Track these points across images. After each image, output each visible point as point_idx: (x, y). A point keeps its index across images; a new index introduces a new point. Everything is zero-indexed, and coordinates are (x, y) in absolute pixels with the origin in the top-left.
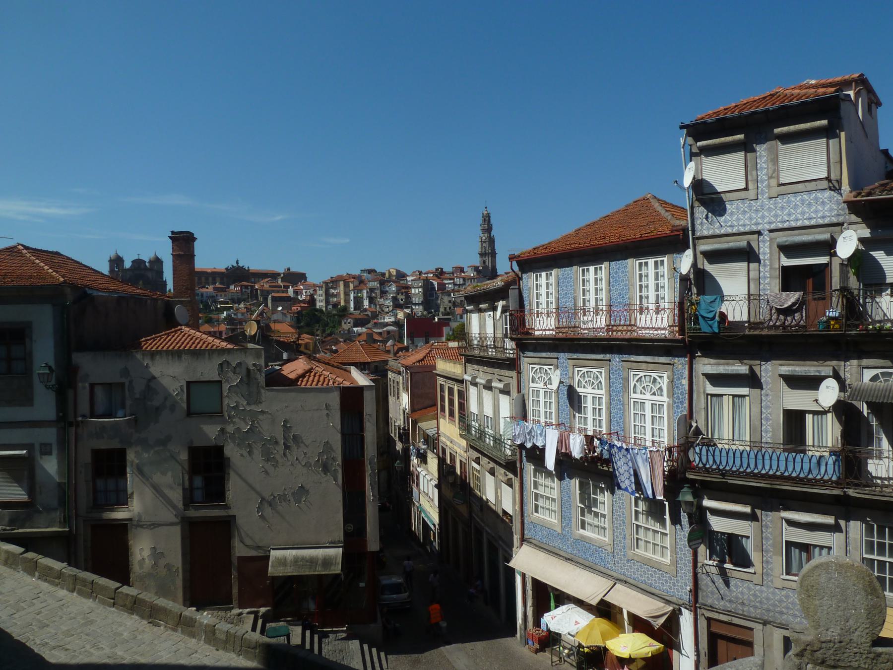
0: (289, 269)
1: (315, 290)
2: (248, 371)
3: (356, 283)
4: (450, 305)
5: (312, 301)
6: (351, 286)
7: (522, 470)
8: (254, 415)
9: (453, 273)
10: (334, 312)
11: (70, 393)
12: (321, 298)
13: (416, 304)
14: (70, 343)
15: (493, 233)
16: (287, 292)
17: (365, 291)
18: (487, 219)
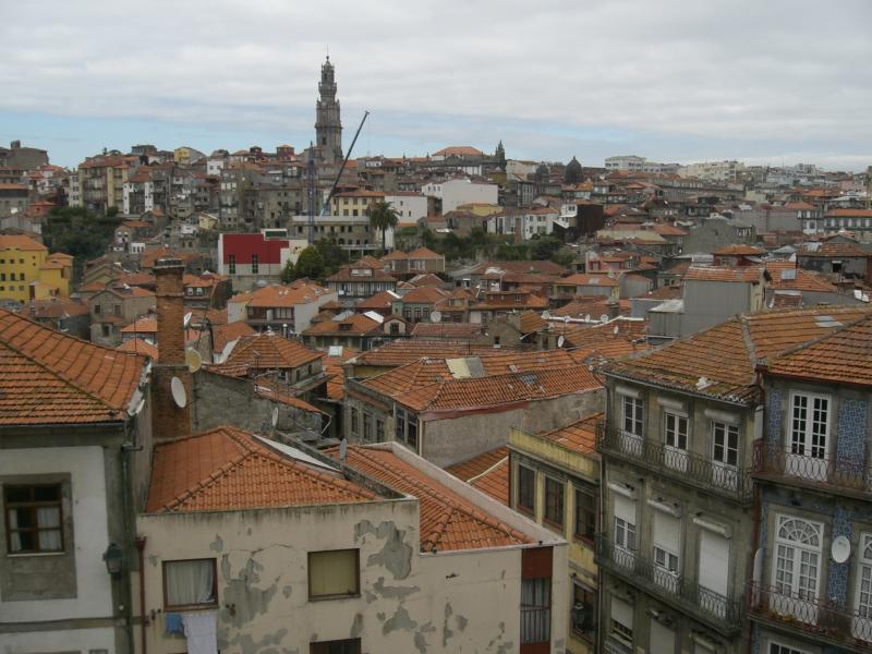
1: (66, 181)
2: (398, 533)
3: (132, 170)
4: (280, 208)
5: (59, 198)
6: (125, 174)
8: (402, 594)
9: (276, 156)
10: (99, 216)
11: (135, 578)
12: (77, 193)
13: (227, 206)
14: (126, 504)
15: (337, 97)
16: (18, 179)
18: (328, 73)
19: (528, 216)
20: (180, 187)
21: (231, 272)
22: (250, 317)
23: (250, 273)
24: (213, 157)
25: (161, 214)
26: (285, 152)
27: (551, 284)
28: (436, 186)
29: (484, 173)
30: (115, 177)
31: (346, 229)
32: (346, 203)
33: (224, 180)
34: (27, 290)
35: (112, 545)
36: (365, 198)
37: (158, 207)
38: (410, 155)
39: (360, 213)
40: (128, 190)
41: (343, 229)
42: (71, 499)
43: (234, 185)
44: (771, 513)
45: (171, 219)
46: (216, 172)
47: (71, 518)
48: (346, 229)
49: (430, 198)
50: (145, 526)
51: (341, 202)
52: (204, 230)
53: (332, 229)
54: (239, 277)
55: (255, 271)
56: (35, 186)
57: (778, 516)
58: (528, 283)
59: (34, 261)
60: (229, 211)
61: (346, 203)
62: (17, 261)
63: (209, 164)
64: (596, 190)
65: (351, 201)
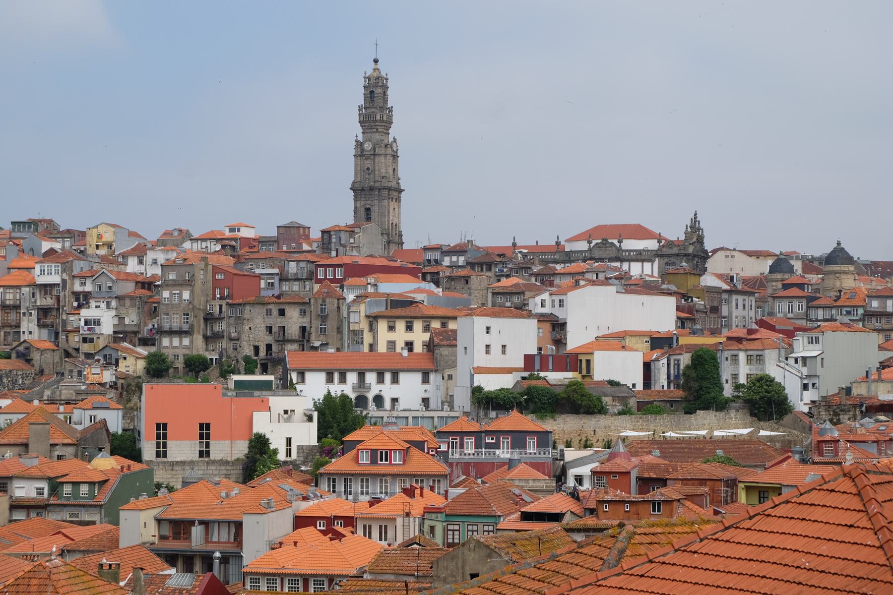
13: (171, 333)
18: (375, 92)
19: (727, 354)
20: (87, 296)
21: (158, 455)
22: (162, 538)
23: (195, 456)
24: (163, 243)
25: (52, 346)
26: (292, 233)
27: (732, 483)
28: (557, 298)
29: (663, 275)
31: (388, 377)
33: (167, 285)
36: (427, 318)
37: (45, 332)
38: (526, 240)
39: (418, 348)
41: (381, 380)
43: (186, 295)
45: (67, 354)
46: (158, 271)
48: (388, 377)
49: (542, 318)
51: (382, 326)
52: (126, 377)
53: (361, 375)
54: (173, 464)
55: (204, 454)
60: (176, 341)
61: (391, 328)
63: (150, 256)
64: (875, 304)
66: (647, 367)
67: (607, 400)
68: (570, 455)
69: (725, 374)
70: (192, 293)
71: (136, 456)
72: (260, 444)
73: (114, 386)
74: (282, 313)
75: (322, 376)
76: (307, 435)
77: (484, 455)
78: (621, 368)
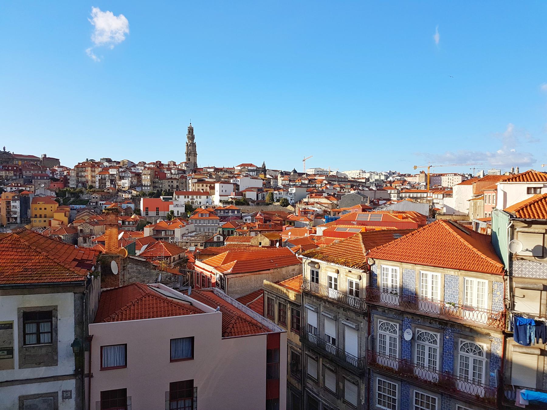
0: (45, 155)
4: (169, 188)
5: (66, 181)
7: (369, 379)
11: (86, 354)
13: (145, 186)
17: (107, 175)
23: (155, 215)
30: (92, 171)
32: (198, 186)
34: (47, 222)
35: (76, 339)
40: (98, 178)
42: (57, 317)
43: (149, 177)
44: (375, 319)
47: (57, 327)
50: (94, 329)
55: (157, 214)
56: (53, 175)
57: (379, 320)
58: (275, 220)
59: (52, 209)
60: (146, 188)
61: (198, 186)
62: (43, 209)
65: (201, 185)
66: (257, 195)
67: (250, 203)
68: (243, 215)
69: (274, 197)
70: (150, 177)
71: (140, 214)
72: (172, 212)
73: (131, 198)
74: (172, 182)
75: (183, 196)
76: (182, 210)
77: (226, 215)
78: (252, 195)
